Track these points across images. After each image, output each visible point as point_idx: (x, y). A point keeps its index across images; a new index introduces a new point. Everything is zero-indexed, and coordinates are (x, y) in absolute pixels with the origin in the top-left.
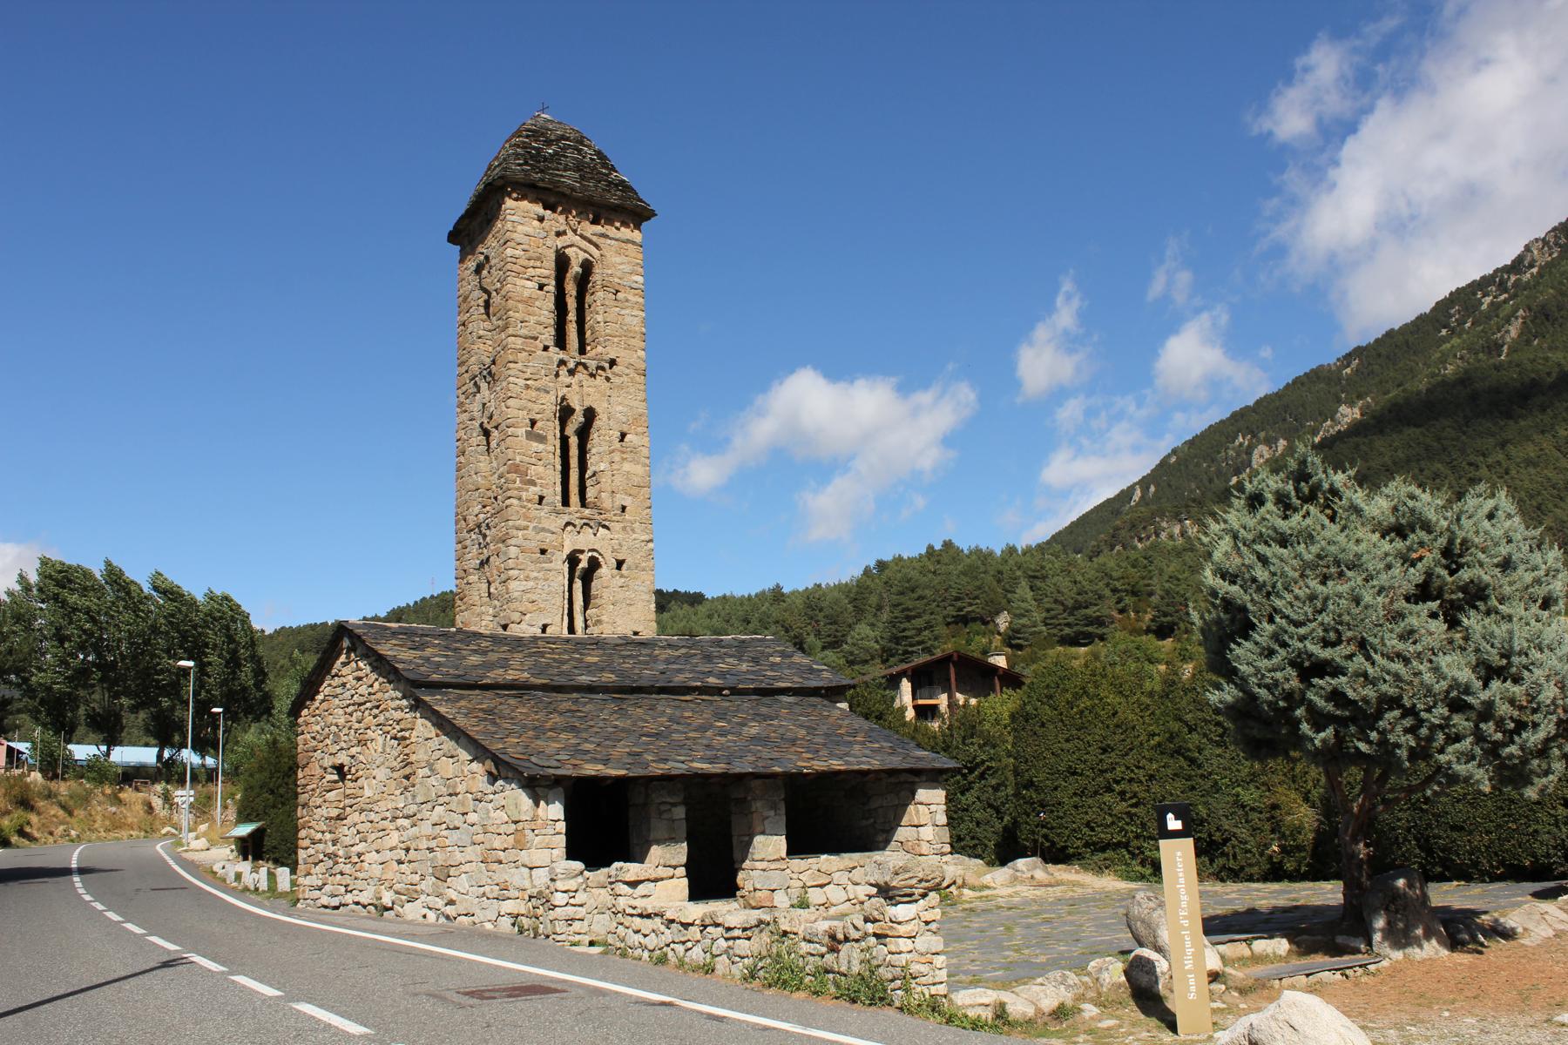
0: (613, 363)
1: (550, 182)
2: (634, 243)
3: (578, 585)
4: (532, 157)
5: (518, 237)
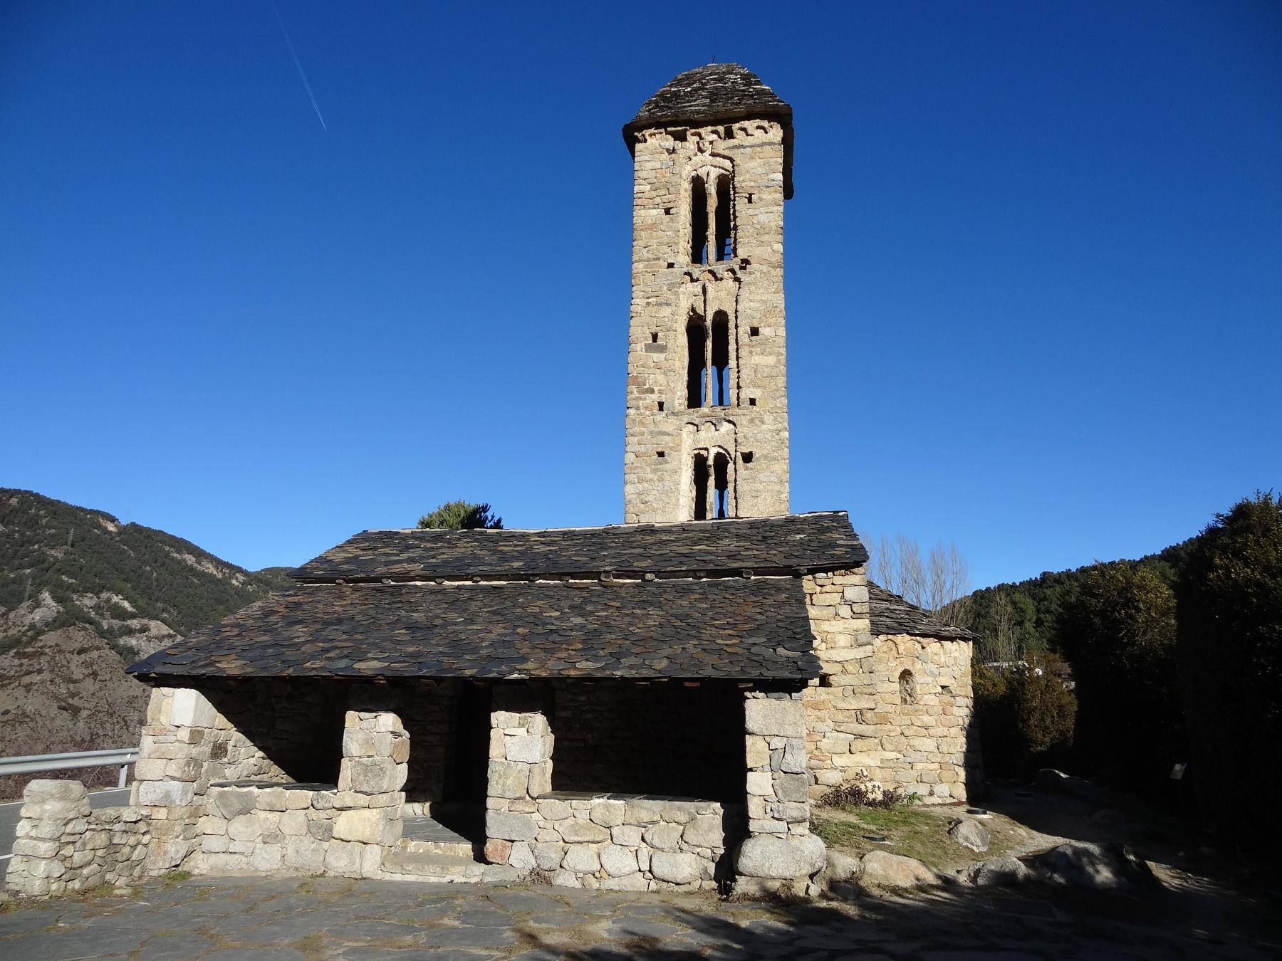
0: (746, 262)
1: (673, 114)
2: (770, 144)
3: (711, 482)
4: (665, 99)
5: (643, 174)
